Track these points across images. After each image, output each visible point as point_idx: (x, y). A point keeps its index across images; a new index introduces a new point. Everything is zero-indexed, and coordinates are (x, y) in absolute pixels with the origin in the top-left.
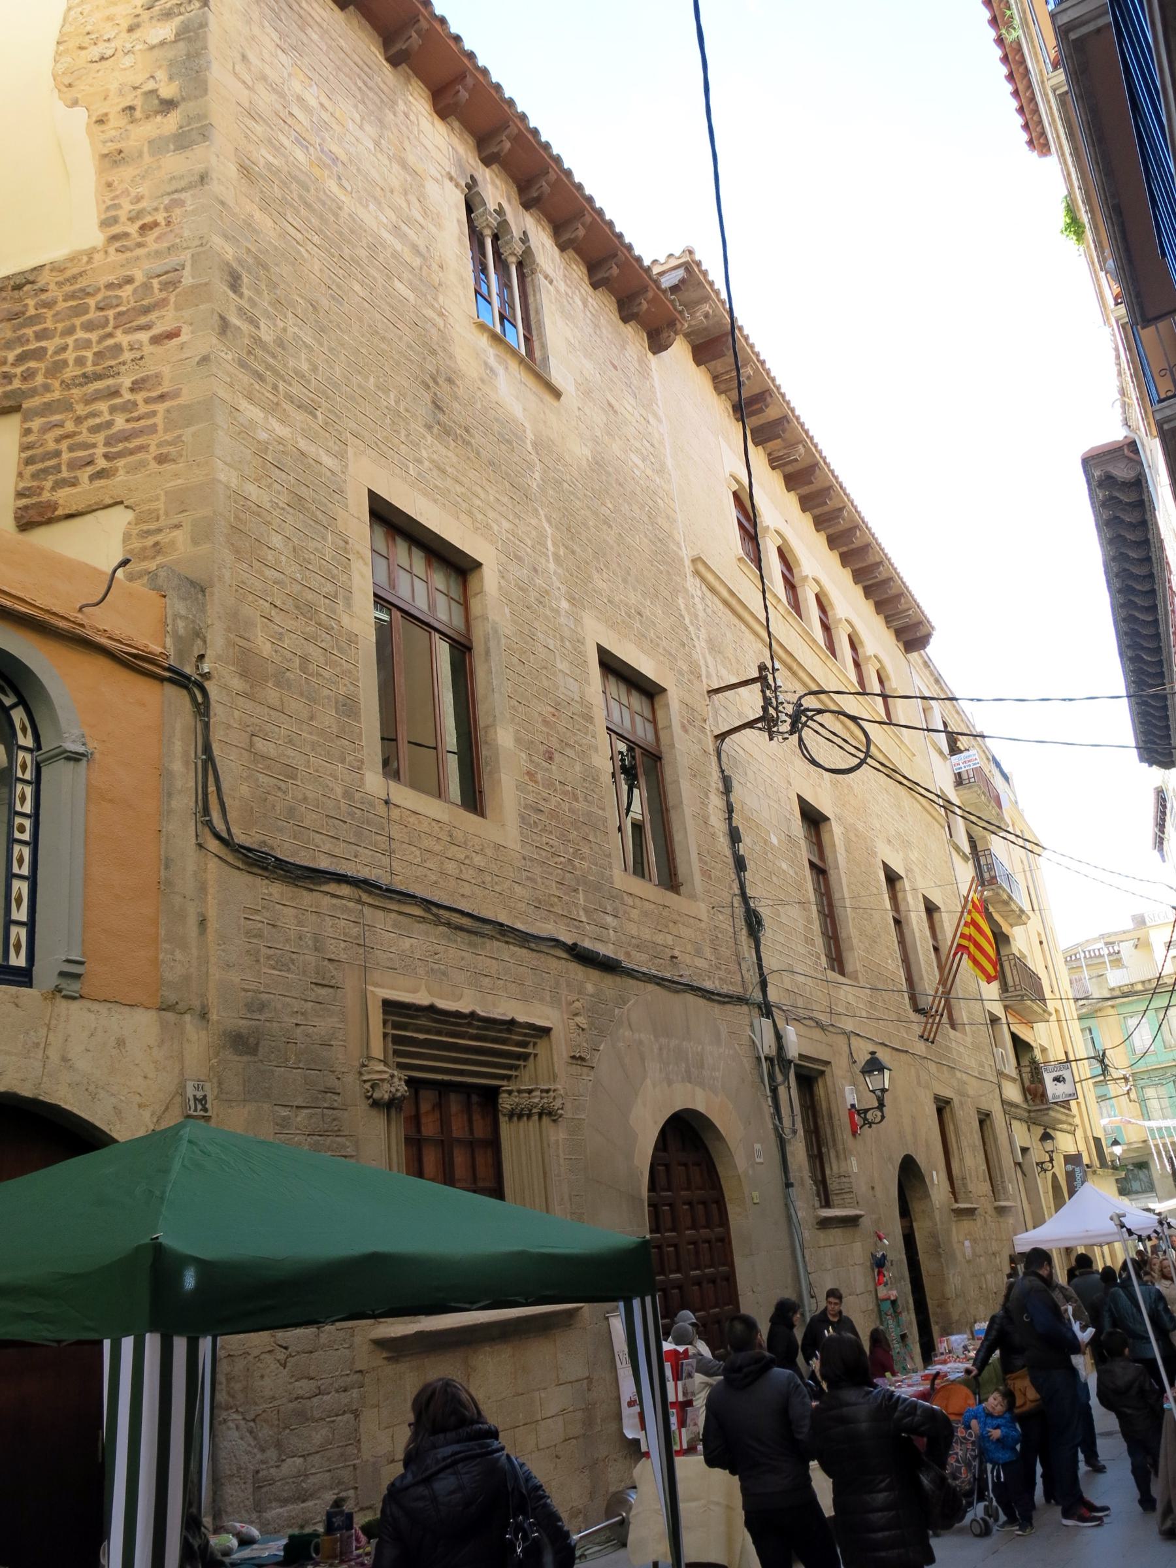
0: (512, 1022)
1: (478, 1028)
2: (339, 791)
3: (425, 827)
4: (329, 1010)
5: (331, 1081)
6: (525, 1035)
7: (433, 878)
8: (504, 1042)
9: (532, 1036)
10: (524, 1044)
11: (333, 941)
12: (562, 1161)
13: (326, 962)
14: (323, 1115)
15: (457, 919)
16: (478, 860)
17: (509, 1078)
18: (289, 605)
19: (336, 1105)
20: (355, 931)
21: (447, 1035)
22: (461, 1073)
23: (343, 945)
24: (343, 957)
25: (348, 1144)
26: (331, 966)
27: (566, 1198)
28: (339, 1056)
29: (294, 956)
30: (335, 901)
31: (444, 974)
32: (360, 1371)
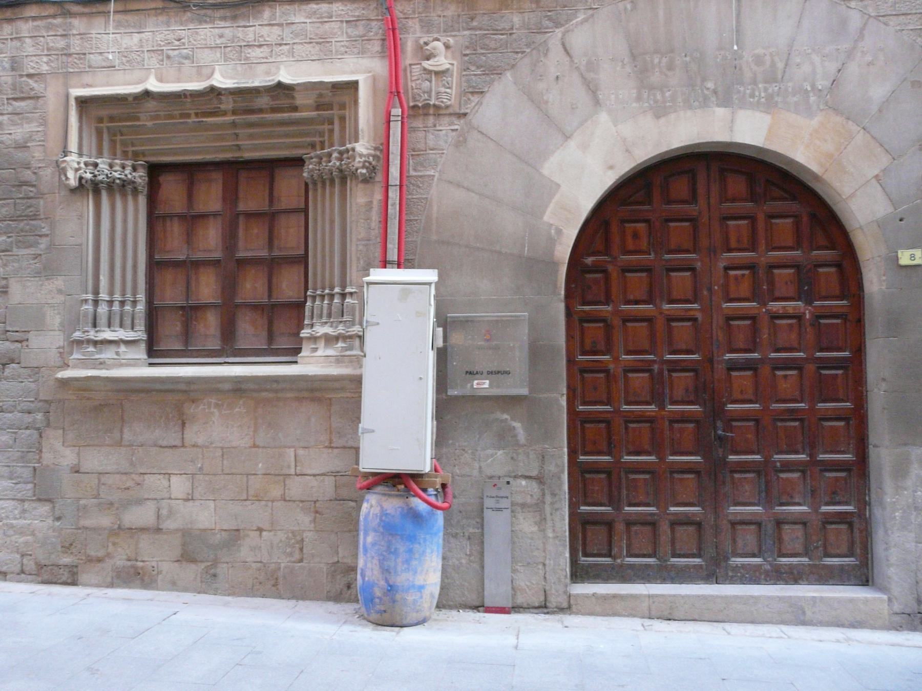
4: (27, 118)
5: (27, 175)
8: (295, 109)
10: (330, 106)
11: (34, 58)
13: (25, 79)
14: (15, 204)
17: (313, 146)
19: (32, 194)
20: (61, 43)
23: (45, 59)
24: (45, 68)
25: (43, 225)
26: (31, 82)
28: (36, 154)
30: (39, 23)
31: (186, 58)
32: (46, 401)
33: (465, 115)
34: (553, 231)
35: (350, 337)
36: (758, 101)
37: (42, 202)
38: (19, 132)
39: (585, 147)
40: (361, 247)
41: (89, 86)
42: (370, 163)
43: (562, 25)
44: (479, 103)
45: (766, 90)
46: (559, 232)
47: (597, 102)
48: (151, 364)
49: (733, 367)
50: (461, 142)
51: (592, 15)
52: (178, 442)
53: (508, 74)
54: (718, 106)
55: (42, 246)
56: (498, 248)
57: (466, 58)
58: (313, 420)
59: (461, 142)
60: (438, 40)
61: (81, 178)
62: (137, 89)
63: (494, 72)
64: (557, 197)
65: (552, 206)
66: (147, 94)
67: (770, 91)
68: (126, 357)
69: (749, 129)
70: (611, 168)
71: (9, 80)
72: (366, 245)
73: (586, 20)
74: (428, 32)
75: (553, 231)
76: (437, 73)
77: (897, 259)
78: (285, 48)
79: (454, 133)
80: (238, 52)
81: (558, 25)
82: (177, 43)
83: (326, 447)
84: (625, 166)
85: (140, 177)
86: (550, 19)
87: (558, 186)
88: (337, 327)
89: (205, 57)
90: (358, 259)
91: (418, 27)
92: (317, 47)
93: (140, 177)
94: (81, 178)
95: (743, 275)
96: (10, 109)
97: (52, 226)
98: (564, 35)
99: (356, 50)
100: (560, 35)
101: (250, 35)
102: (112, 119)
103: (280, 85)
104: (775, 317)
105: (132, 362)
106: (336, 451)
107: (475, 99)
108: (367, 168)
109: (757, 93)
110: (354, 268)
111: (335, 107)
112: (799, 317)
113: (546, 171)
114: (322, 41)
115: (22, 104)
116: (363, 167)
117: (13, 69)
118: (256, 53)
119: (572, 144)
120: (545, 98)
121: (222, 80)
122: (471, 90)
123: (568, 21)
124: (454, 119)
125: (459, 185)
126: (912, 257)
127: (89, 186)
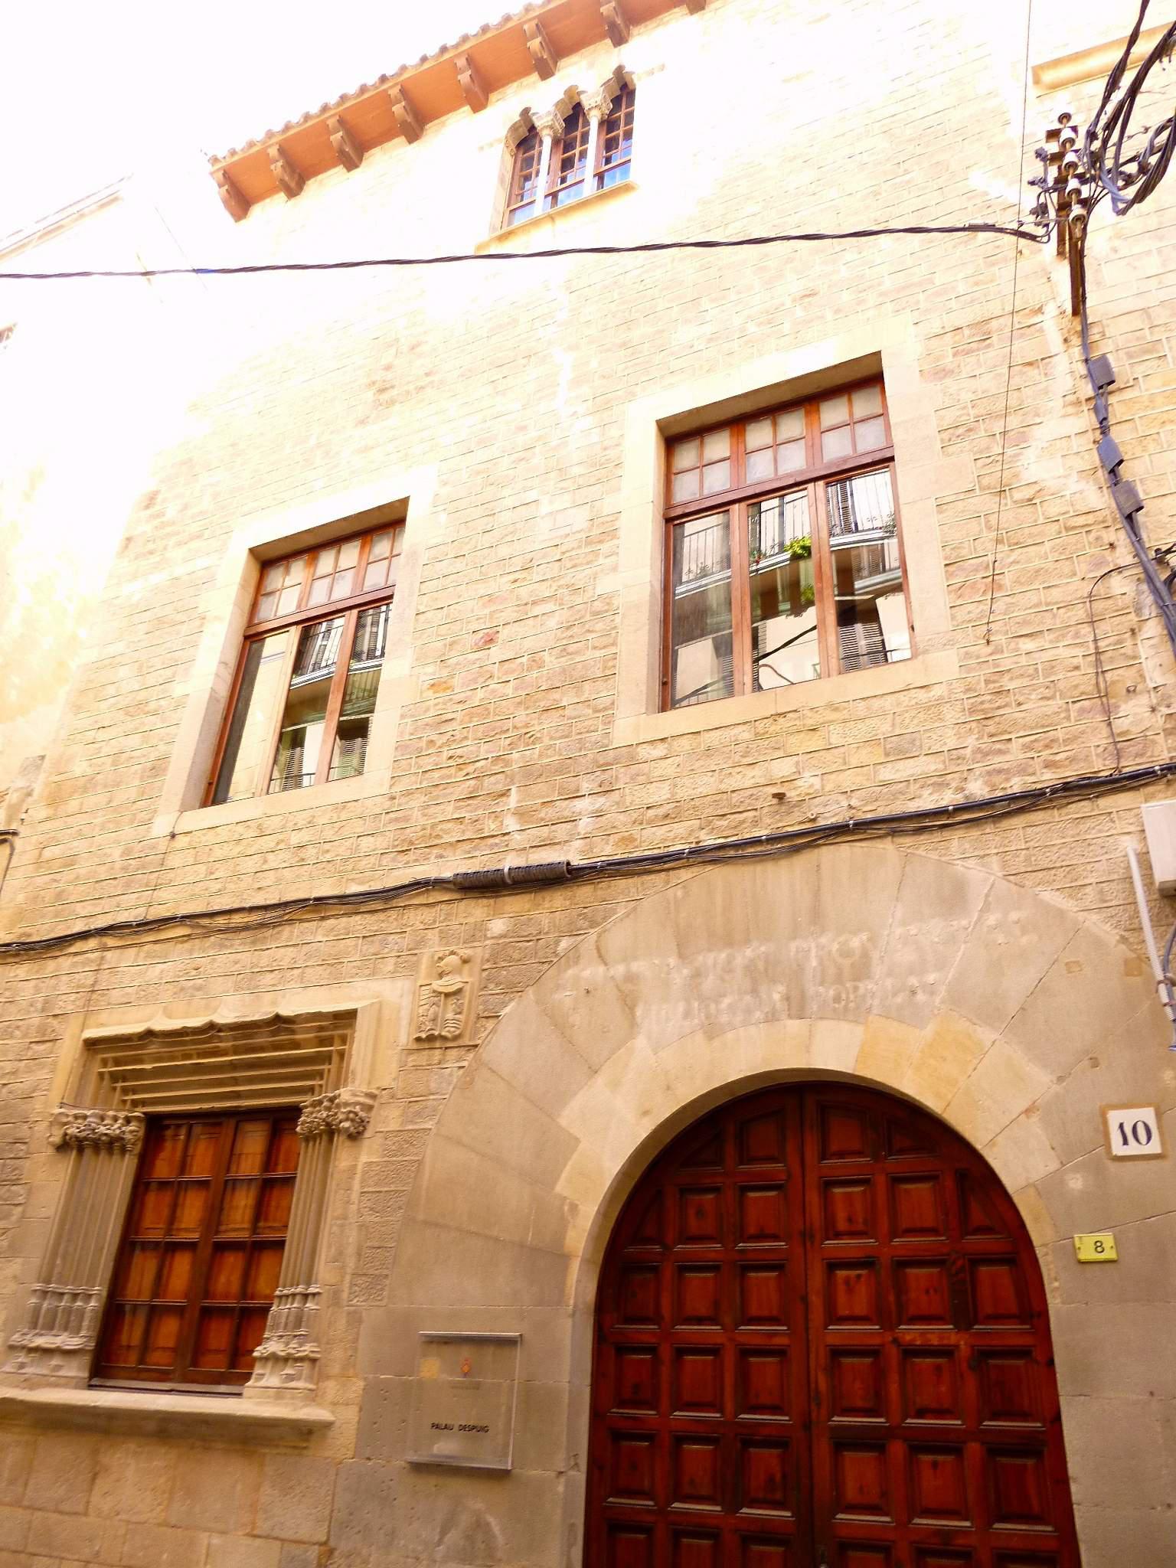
0: (279, 1022)
1: (235, 1039)
2: (116, 854)
3: (223, 834)
5: (24, 1131)
6: (321, 1029)
7: (219, 886)
8: (296, 1045)
9: (336, 1028)
10: (329, 1041)
12: (355, 1196)
15: (238, 919)
16: (295, 839)
17: (311, 1090)
18: (121, 715)
19: (21, 1154)
21: (200, 1055)
22: (237, 1095)
27: (351, 1250)
29: (20, 1023)
33: (476, 1046)
34: (566, 1208)
35: (301, 1359)
36: (846, 1008)
37: (27, 1163)
38: (28, 1081)
39: (615, 1085)
40: (335, 1229)
41: (102, 1025)
42: (356, 1114)
43: (598, 924)
44: (493, 1031)
45: (856, 989)
46: (574, 1208)
47: (633, 1024)
48: (91, 1387)
49: (845, 1441)
50: (467, 1084)
51: (635, 909)
52: (81, 1508)
53: (530, 991)
54: (790, 1017)
55: (14, 1218)
56: (495, 1234)
57: (485, 974)
58: (239, 1487)
59: (467, 1084)
60: (453, 953)
61: (66, 1134)
62: (139, 1028)
63: (513, 989)
64: (575, 1156)
65: (568, 1168)
66: (150, 1034)
67: (861, 991)
68: (61, 1373)
69: (833, 1049)
70: (646, 1113)
71: (36, 1021)
72: (342, 1226)
73: (627, 915)
74: (447, 944)
75: (566, 1208)
76: (447, 995)
77: (1075, 1250)
78: (296, 972)
79: (461, 1071)
80: (248, 981)
81: (593, 924)
82: (194, 972)
83: (247, 1535)
84: (665, 1109)
85: (133, 1131)
86: (585, 916)
87: (577, 1140)
88: (287, 1344)
89: (218, 985)
90: (329, 1246)
91: (437, 938)
92: (329, 969)
93: (131, 1132)
94: (66, 1134)
95: (859, 1276)
96: (30, 1054)
97: (30, 1192)
98: (599, 936)
99: (367, 972)
100: (594, 937)
101: (264, 959)
102: (117, 1062)
103: (278, 1019)
104: (910, 1352)
105: (62, 1381)
106: (258, 1541)
107: (490, 1024)
108: (352, 1120)
109: (844, 996)
110: (323, 1257)
111: (337, 1041)
112: (947, 1352)
113: (563, 1121)
114: (333, 963)
115: (42, 1047)
116: (347, 1119)
117: (43, 1010)
118: (269, 978)
119: (600, 1080)
120: (571, 1020)
121: (227, 1014)
122: (486, 1014)
123: (605, 919)
124: (463, 1051)
125: (459, 1143)
126: (1099, 1246)
127: (74, 1143)
